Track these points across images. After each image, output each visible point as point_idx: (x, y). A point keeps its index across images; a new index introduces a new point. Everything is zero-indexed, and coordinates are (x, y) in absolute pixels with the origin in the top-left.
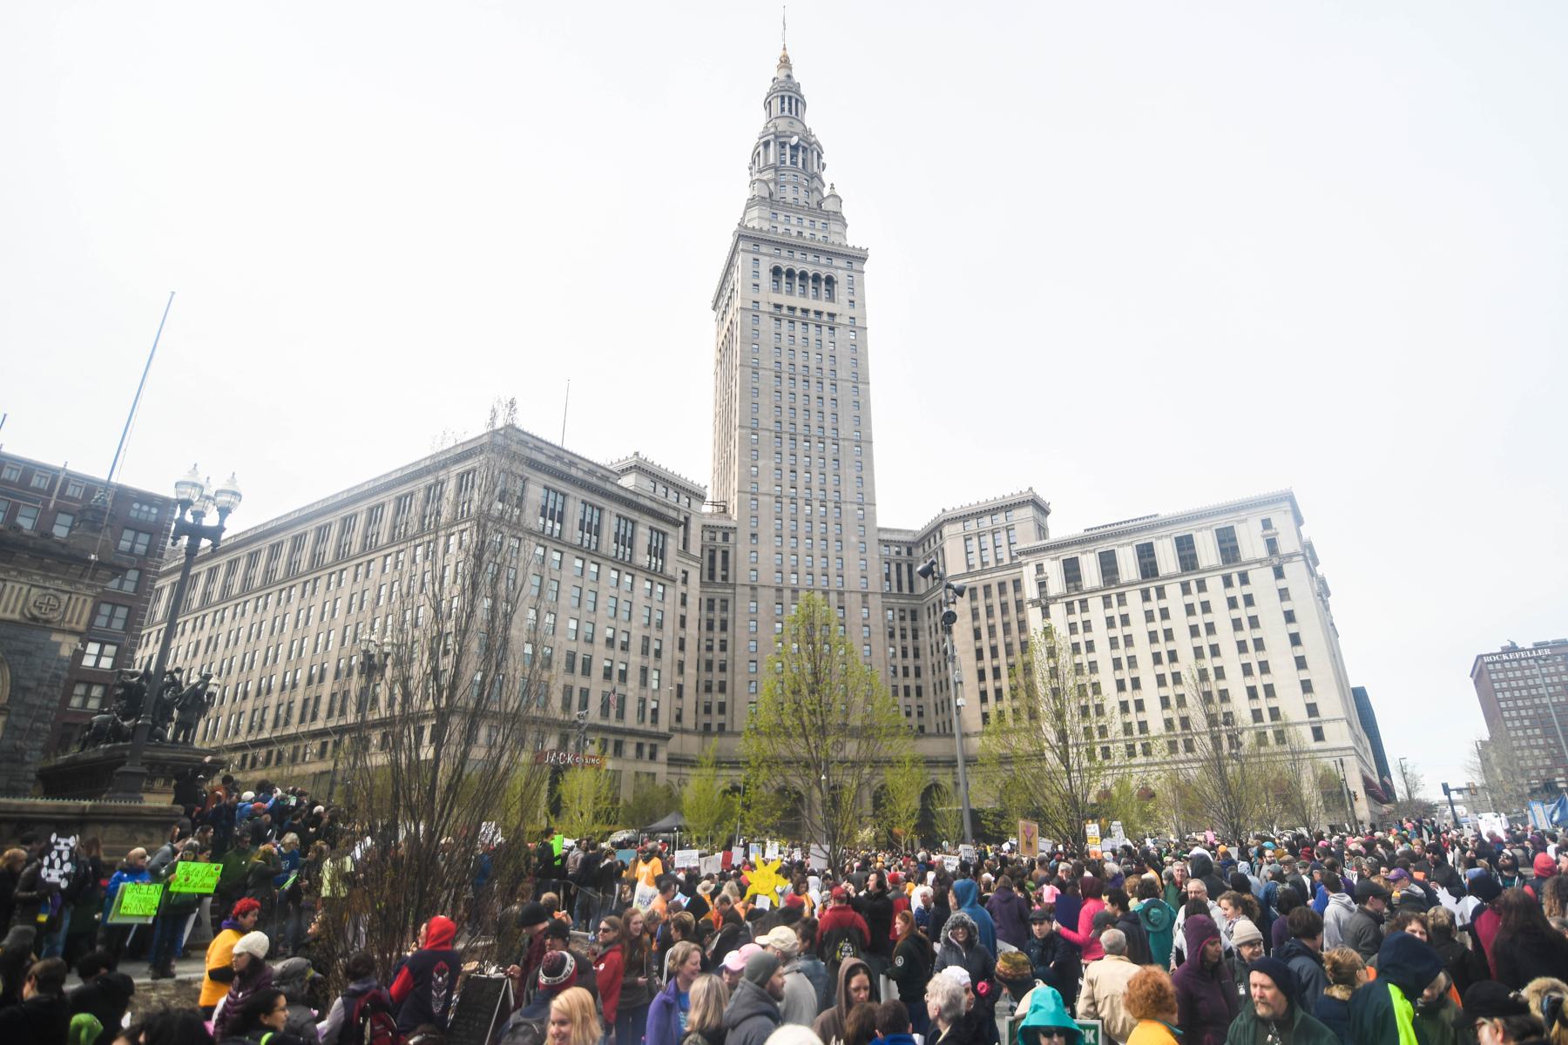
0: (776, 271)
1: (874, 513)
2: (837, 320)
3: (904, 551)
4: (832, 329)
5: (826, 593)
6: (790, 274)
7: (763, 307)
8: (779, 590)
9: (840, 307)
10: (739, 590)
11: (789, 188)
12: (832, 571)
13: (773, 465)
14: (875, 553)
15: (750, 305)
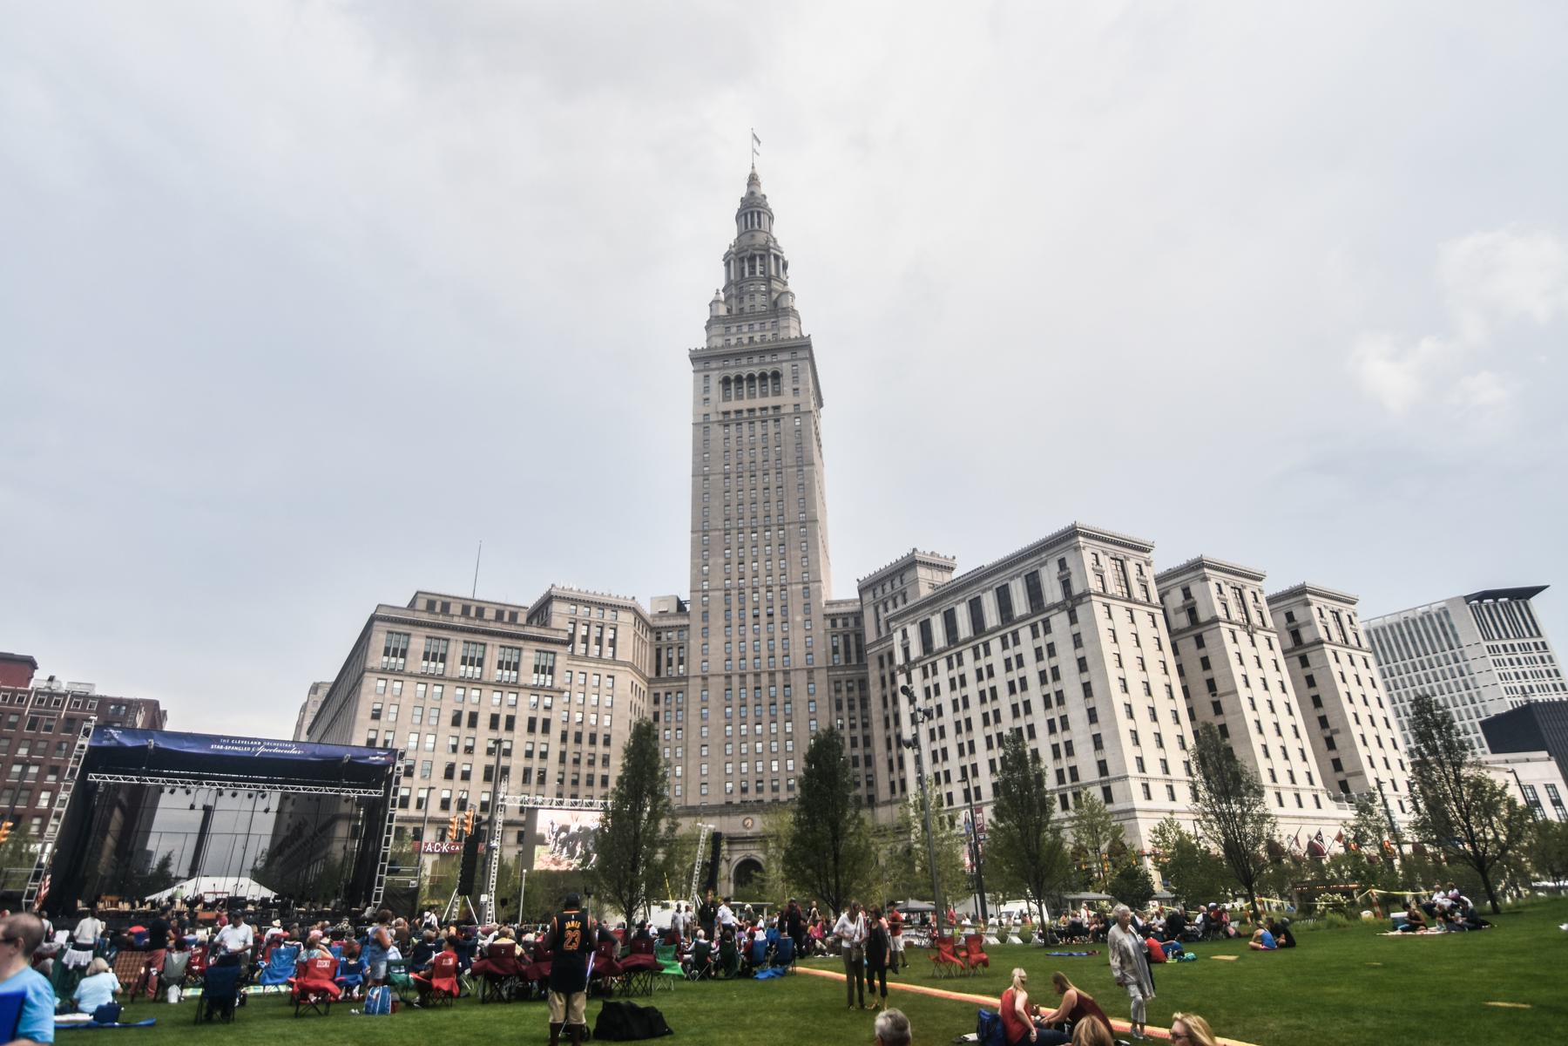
0: (726, 382)
1: (819, 589)
2: (783, 411)
3: (851, 622)
4: (777, 420)
5: (772, 674)
6: (739, 379)
7: (713, 418)
8: (728, 677)
9: (787, 400)
10: (691, 681)
11: (746, 298)
12: (779, 652)
13: (722, 560)
14: (821, 627)
15: (701, 419)
